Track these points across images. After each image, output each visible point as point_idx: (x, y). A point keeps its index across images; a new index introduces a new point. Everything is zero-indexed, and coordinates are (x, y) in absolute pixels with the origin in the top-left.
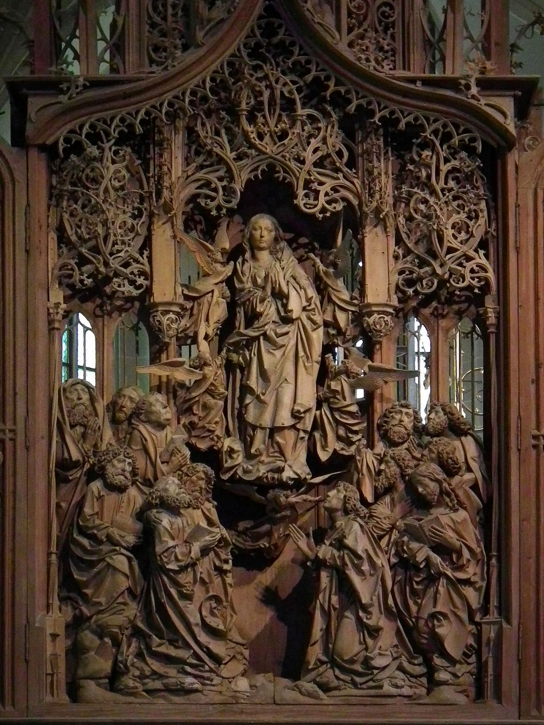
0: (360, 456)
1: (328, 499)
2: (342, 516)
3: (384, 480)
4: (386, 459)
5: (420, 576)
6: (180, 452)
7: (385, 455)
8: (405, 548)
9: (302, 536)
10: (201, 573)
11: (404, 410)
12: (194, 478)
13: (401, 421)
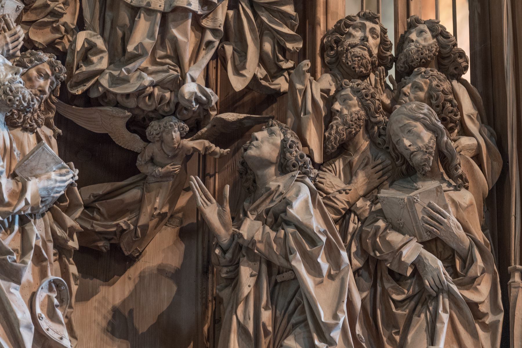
0: (302, 83)
1: (255, 143)
2: (276, 175)
3: (341, 127)
4: (343, 93)
5: (404, 293)
6: (9, 29)
7: (340, 88)
8: (378, 240)
9: (209, 200)
10: (37, 237)
11: (369, 25)
12: (33, 72)
13: (365, 39)
